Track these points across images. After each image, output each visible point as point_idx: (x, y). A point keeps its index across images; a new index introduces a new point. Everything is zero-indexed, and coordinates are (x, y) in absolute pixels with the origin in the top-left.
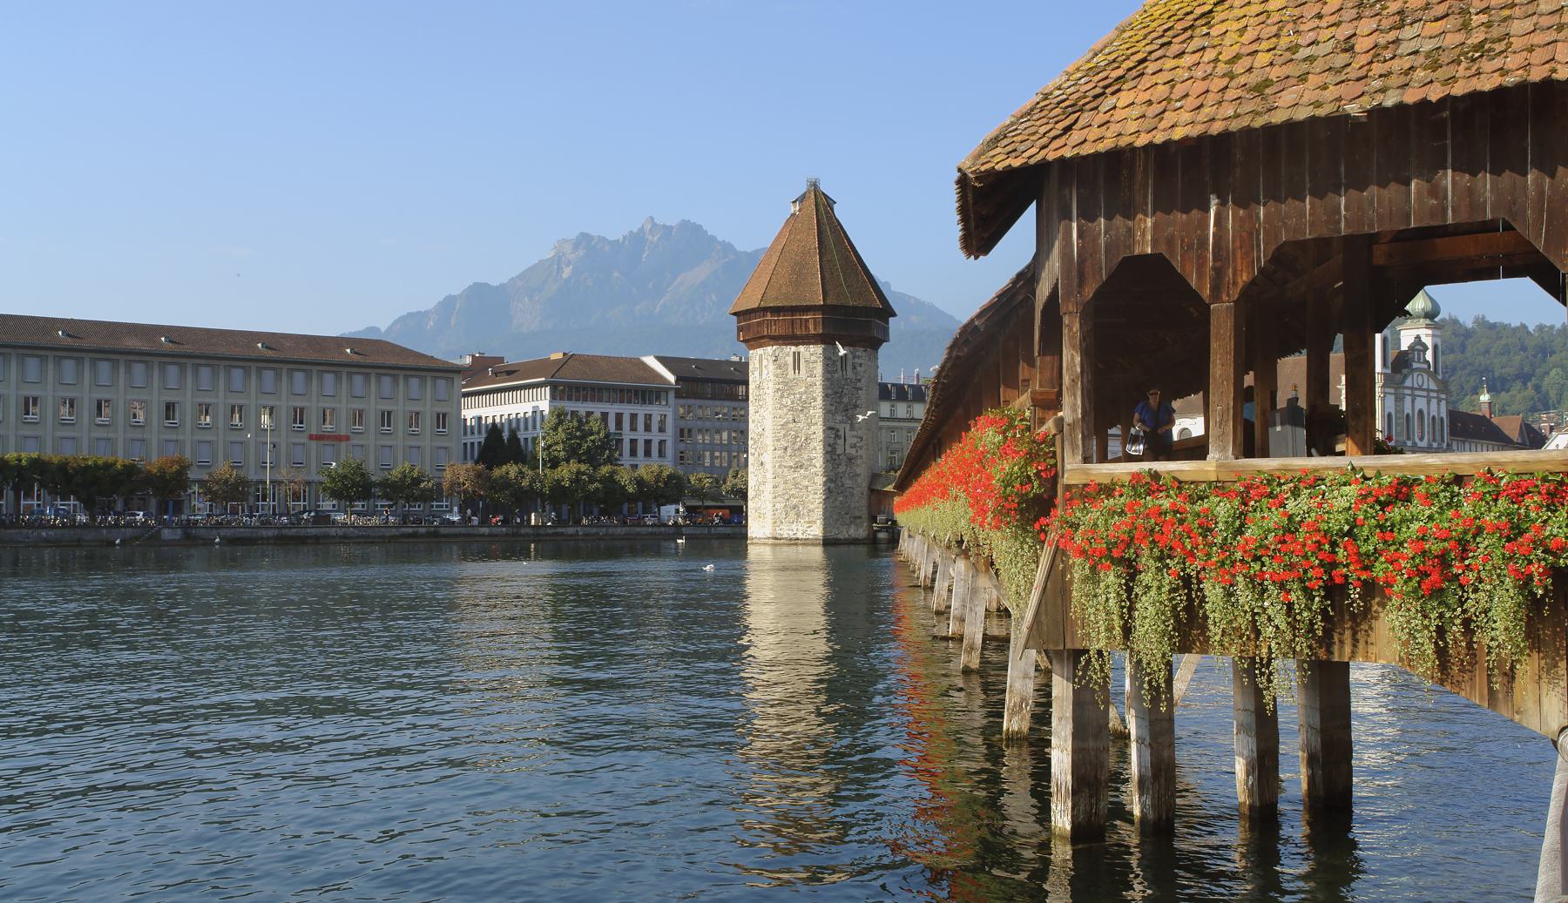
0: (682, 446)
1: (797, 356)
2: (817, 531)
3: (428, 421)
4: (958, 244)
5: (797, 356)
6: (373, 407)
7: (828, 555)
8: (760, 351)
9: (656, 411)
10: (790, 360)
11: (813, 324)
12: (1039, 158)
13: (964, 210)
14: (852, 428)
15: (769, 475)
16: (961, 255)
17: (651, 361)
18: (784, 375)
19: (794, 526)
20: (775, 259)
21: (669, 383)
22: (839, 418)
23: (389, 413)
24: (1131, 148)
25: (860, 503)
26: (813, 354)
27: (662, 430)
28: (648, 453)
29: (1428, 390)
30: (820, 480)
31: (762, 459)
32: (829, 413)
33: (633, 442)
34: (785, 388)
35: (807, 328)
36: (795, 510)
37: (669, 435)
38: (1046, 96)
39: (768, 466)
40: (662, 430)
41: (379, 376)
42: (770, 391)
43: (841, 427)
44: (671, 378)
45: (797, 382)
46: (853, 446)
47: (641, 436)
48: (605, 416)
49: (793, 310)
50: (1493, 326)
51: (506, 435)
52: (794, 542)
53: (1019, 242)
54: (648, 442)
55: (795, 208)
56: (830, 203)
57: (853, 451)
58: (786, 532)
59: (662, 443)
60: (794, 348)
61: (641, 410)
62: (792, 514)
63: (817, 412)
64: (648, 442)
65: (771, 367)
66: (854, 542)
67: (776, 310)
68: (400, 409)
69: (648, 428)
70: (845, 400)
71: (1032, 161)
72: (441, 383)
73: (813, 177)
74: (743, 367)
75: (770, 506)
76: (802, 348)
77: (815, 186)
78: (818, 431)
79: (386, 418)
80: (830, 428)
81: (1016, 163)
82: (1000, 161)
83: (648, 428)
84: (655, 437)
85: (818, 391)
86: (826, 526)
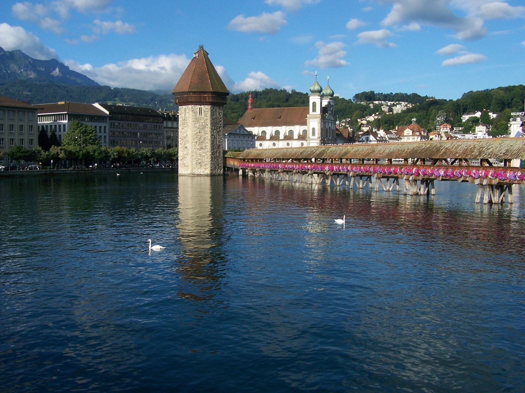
0: (112, 138)
1: (200, 109)
2: (208, 171)
3: (6, 127)
5: (200, 109)
6: (16, 124)
7: (211, 180)
8: (184, 107)
9: (103, 125)
11: (208, 97)
15: (190, 151)
17: (97, 105)
18: (196, 115)
19: (199, 170)
20: (191, 73)
23: (12, 125)
25: (221, 161)
26: (207, 109)
27: (105, 132)
29: (332, 120)
34: (196, 120)
35: (206, 99)
36: (200, 164)
37: (107, 134)
40: (105, 132)
41: (18, 111)
42: (190, 121)
44: (107, 113)
45: (201, 119)
48: (96, 127)
49: (201, 93)
50: (298, 93)
51: (49, 134)
52: (199, 175)
55: (194, 56)
58: (197, 172)
59: (105, 137)
60: (199, 106)
61: (98, 125)
62: (199, 166)
63: (208, 129)
65: (191, 113)
66: (219, 175)
67: (194, 92)
68: (16, 124)
69: (100, 132)
72: (30, 114)
73: (201, 44)
75: (190, 163)
76: (202, 106)
77: (202, 47)
78: (209, 136)
79: (12, 127)
83: (100, 132)
84: (103, 134)
85: (209, 122)
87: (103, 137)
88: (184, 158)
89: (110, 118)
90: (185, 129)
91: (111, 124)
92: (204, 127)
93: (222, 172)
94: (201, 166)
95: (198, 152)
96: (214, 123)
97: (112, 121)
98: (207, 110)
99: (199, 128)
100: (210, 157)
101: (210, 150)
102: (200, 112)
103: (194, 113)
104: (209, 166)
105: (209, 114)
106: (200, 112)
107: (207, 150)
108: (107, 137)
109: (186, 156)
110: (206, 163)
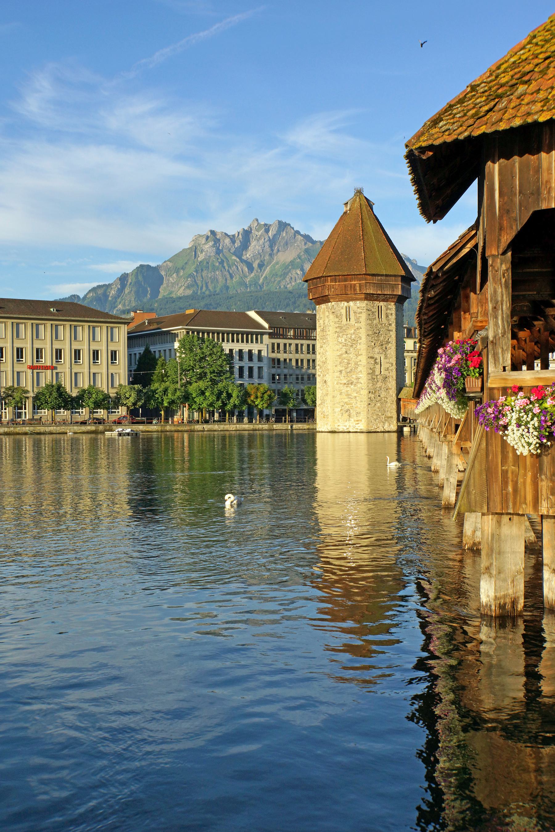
1: (348, 309)
4: (418, 211)
5: (348, 309)
10: (343, 312)
12: (466, 134)
13: (416, 181)
14: (386, 357)
16: (422, 219)
17: (252, 314)
19: (347, 424)
21: (263, 328)
22: (376, 350)
24: (536, 123)
26: (358, 306)
28: (251, 376)
30: (365, 392)
31: (325, 378)
32: (371, 347)
33: (241, 369)
35: (355, 290)
38: (473, 88)
39: (329, 383)
43: (377, 356)
44: (266, 325)
46: (387, 369)
47: (246, 363)
49: (346, 277)
53: (466, 208)
54: (251, 369)
56: (370, 205)
57: (386, 373)
59: (260, 368)
60: (346, 304)
61: (246, 347)
63: (362, 346)
64: (251, 369)
65: (331, 316)
70: (382, 338)
71: (461, 137)
73: (359, 186)
74: (313, 318)
76: (351, 304)
77: (359, 192)
78: (363, 360)
80: (372, 358)
81: (449, 139)
82: (439, 138)
84: (255, 364)
85: (363, 333)
86: (369, 422)
87: (256, 371)
88: (323, 402)
89: (271, 335)
90: (324, 346)
91: (273, 344)
92: (354, 342)
93: (394, 427)
94: (349, 416)
95: (344, 389)
96: (375, 334)
97: (276, 341)
98: (359, 310)
99: (345, 345)
100: (365, 398)
101: (364, 386)
102: (348, 317)
103: (337, 317)
104: (363, 417)
105: (363, 317)
106: (348, 317)
107: (359, 385)
108: (265, 370)
109: (326, 398)
110: (358, 410)
